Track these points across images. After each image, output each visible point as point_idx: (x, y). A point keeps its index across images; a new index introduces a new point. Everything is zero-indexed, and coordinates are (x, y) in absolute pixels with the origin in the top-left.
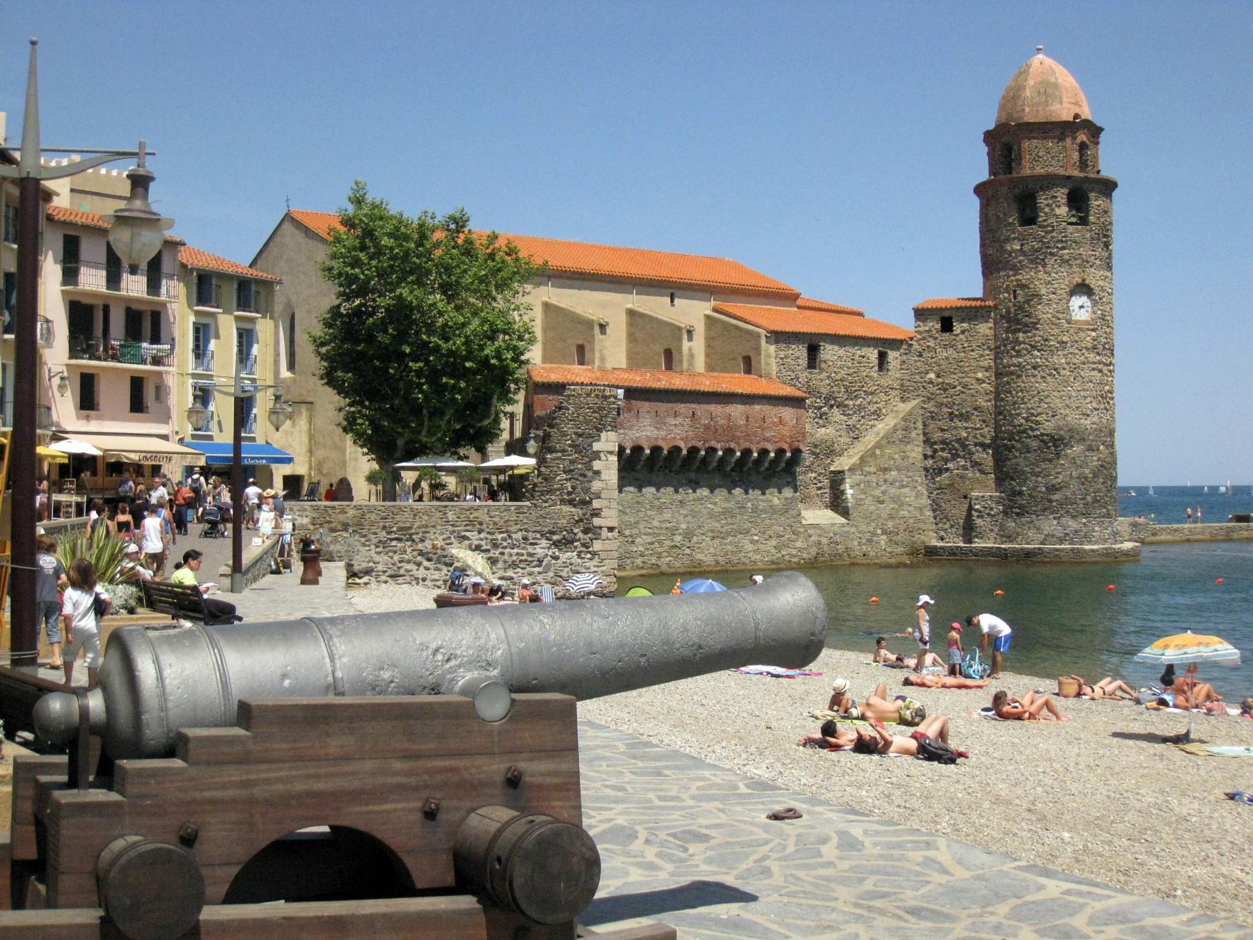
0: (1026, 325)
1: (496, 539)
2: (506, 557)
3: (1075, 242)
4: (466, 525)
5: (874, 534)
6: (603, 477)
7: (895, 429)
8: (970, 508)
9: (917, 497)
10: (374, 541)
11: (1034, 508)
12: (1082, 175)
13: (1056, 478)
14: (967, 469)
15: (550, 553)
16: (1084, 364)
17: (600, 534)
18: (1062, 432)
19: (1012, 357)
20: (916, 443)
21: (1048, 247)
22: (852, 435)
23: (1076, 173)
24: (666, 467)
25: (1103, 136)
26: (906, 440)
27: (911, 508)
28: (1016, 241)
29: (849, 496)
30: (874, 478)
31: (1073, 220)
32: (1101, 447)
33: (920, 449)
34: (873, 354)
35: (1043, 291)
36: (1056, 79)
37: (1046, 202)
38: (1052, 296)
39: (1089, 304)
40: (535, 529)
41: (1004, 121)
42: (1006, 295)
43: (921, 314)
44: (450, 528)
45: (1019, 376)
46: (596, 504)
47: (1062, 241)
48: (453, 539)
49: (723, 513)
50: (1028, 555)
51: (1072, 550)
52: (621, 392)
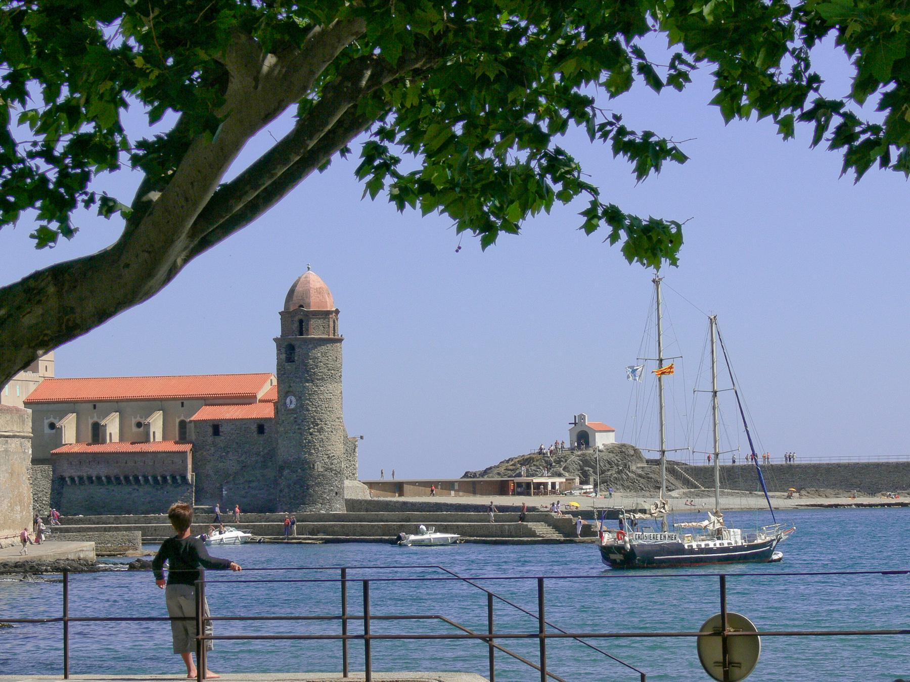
30: (241, 486)
32: (299, 470)
34: (254, 427)
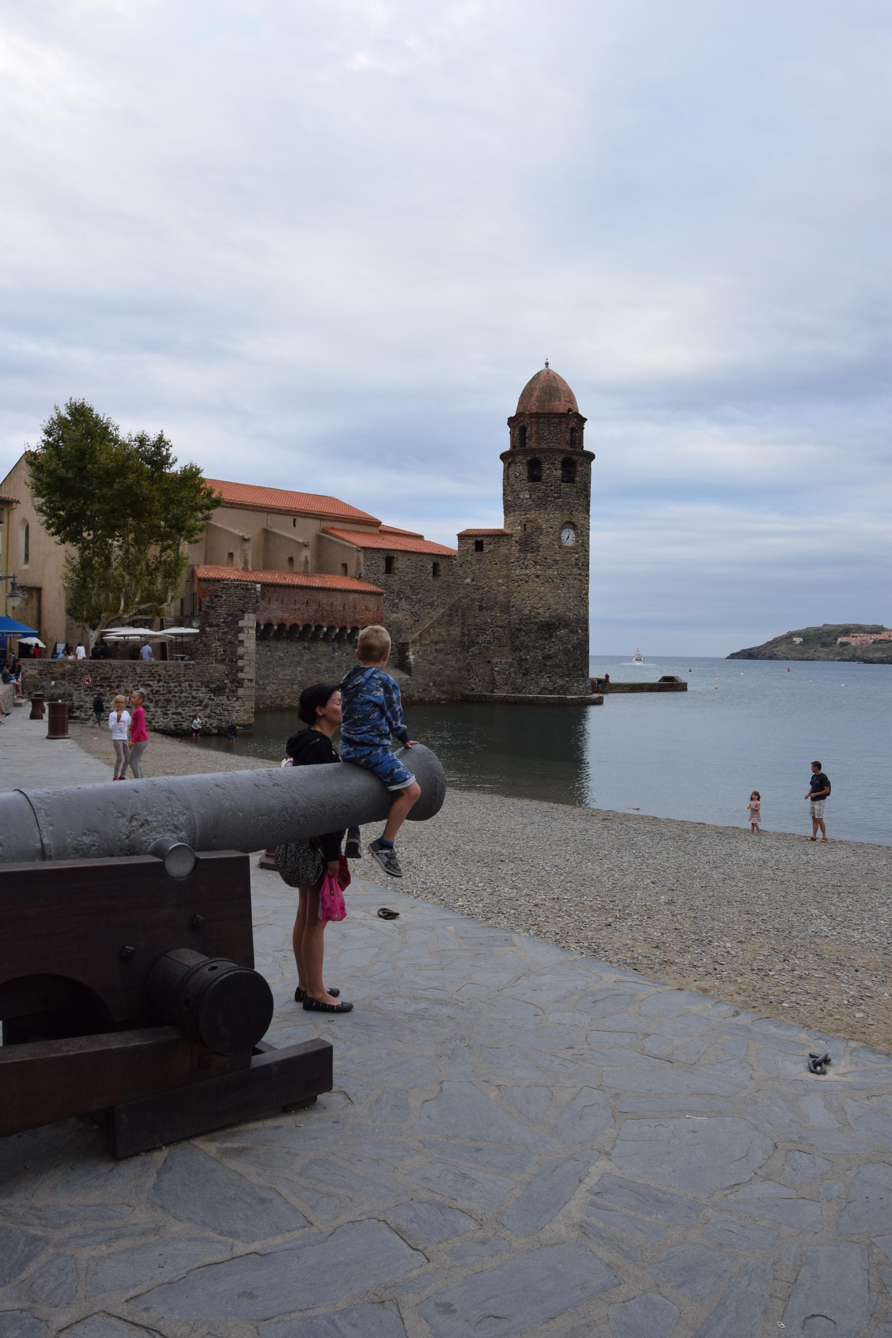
0: (532, 548)
1: (170, 687)
2: (177, 699)
3: (566, 493)
4: (149, 677)
5: (428, 685)
6: (246, 644)
7: (443, 615)
8: (492, 670)
9: (457, 662)
10: (83, 687)
11: (535, 670)
12: (572, 450)
13: (549, 651)
14: (491, 643)
15: (208, 697)
16: (570, 575)
17: (243, 684)
18: (553, 620)
19: (522, 569)
20: (456, 625)
21: (548, 497)
22: (414, 618)
23: (568, 448)
24: (288, 638)
25: (586, 425)
26: (450, 623)
27: (453, 669)
28: (527, 492)
29: (412, 660)
31: (566, 479)
33: (460, 629)
34: (430, 566)
35: (543, 527)
36: (557, 385)
37: (548, 466)
38: (549, 529)
39: (574, 535)
40: (198, 680)
41: (521, 411)
42: (519, 528)
43: (462, 537)
44: (138, 679)
45: (527, 582)
46: (240, 663)
47: (557, 493)
48: (140, 686)
49: (327, 670)
50: (531, 702)
51: (559, 698)
52: (258, 586)
